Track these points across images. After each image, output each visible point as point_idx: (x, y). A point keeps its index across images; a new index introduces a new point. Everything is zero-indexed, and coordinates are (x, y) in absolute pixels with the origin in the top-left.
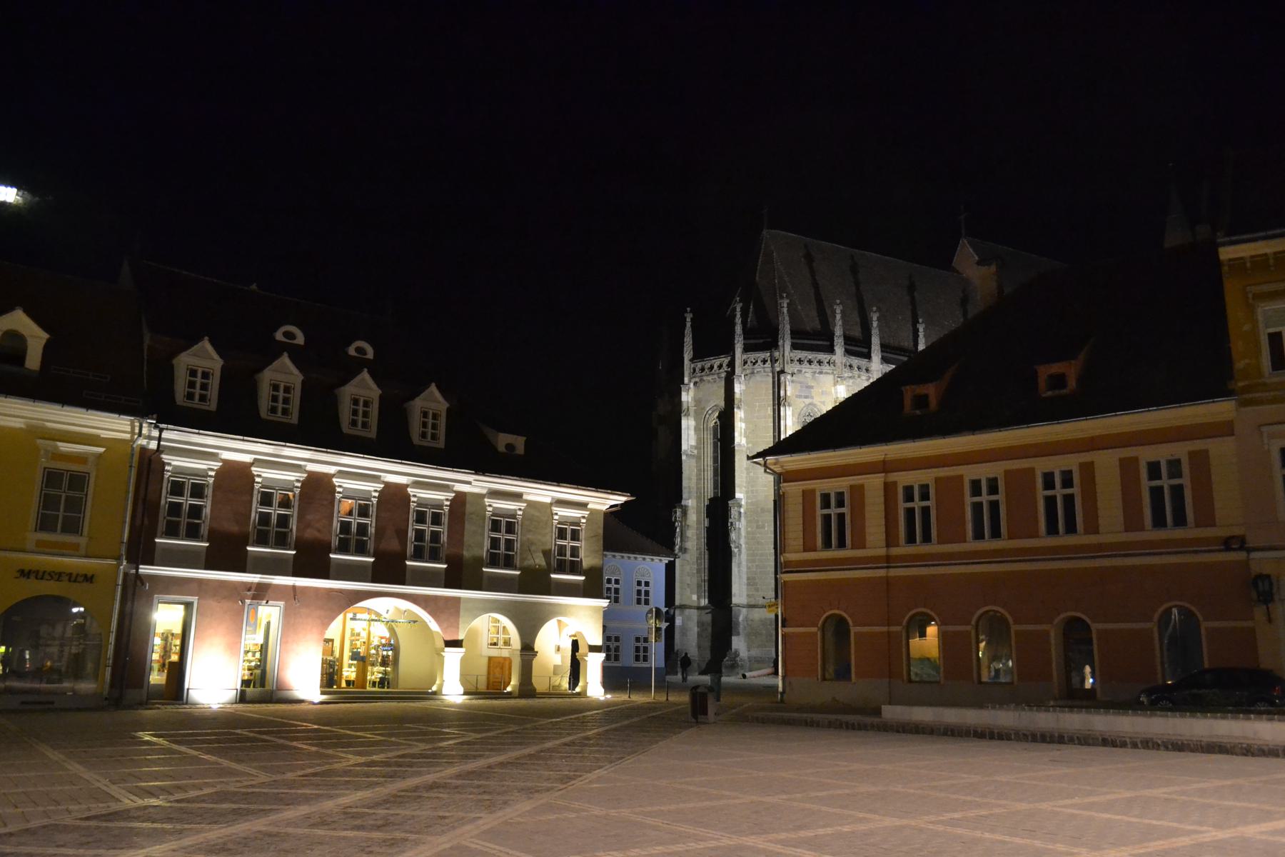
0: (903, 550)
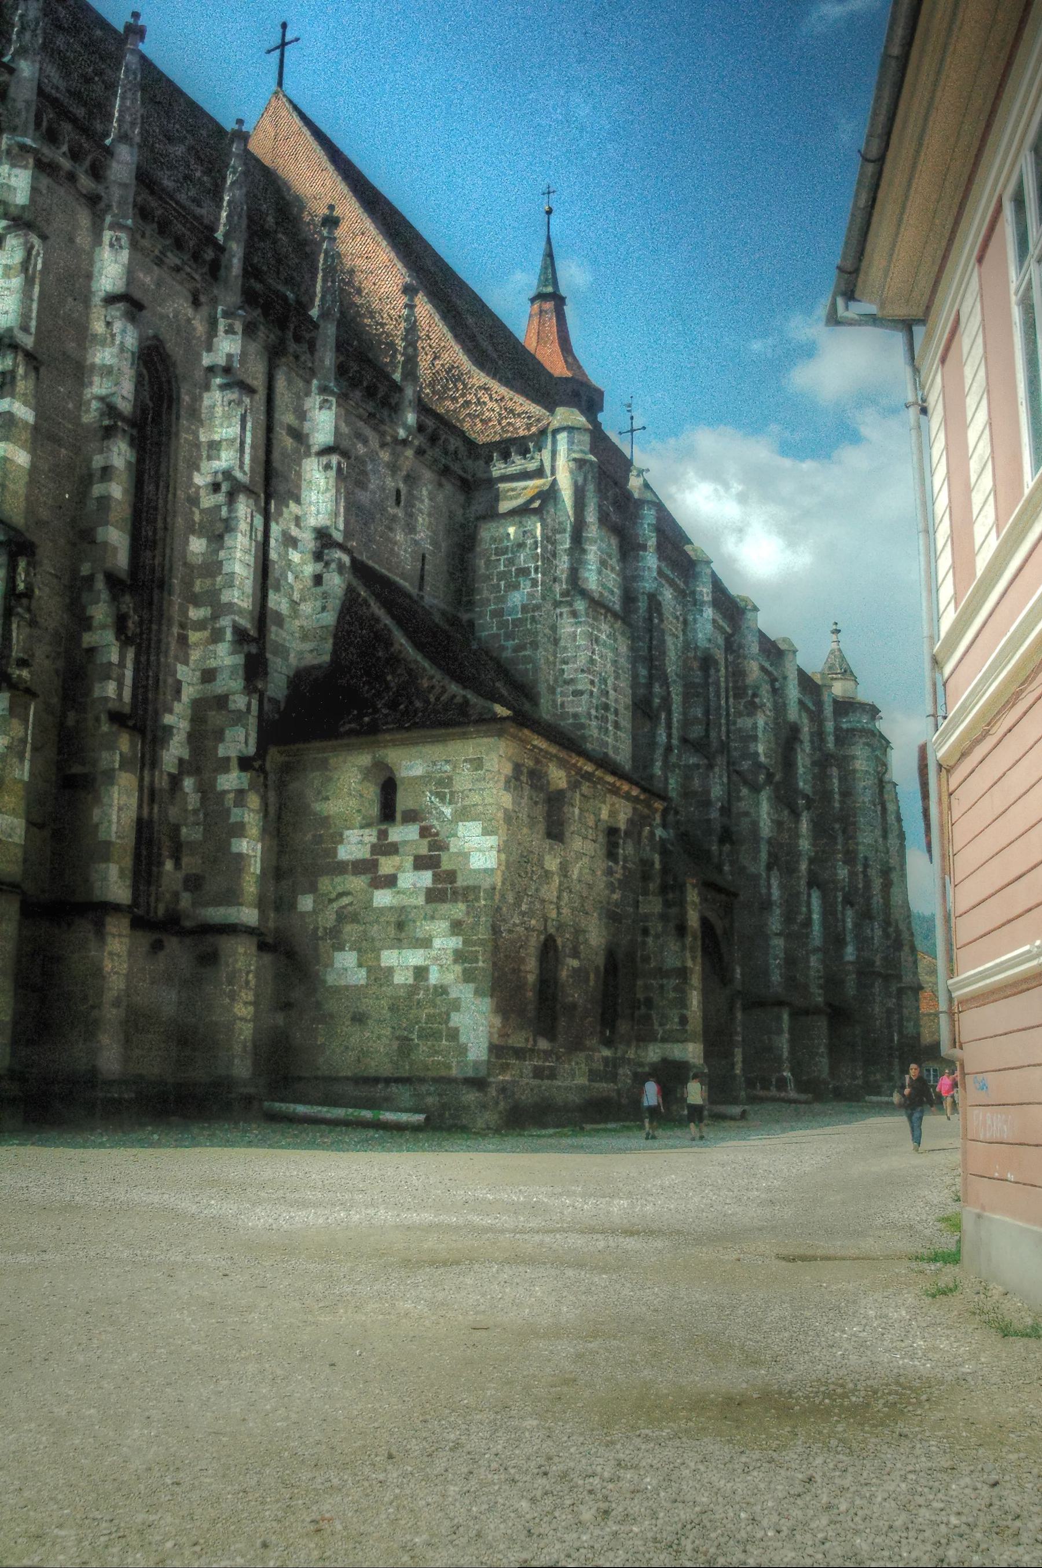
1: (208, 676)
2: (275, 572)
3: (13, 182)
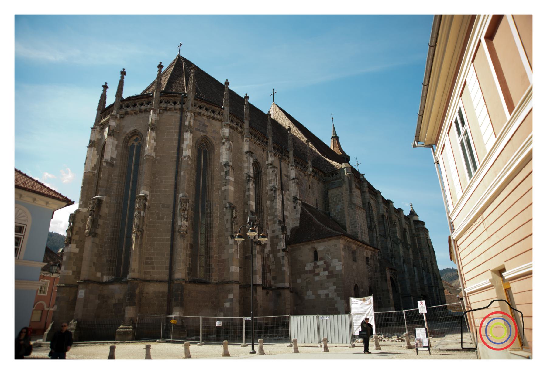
2: (285, 207)
3: (226, 131)
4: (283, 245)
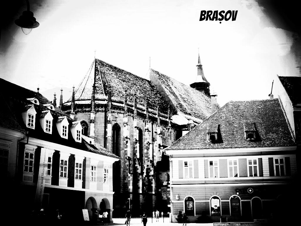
0: (210, 179)
1: (148, 166)
2: (154, 151)
4: (152, 173)
